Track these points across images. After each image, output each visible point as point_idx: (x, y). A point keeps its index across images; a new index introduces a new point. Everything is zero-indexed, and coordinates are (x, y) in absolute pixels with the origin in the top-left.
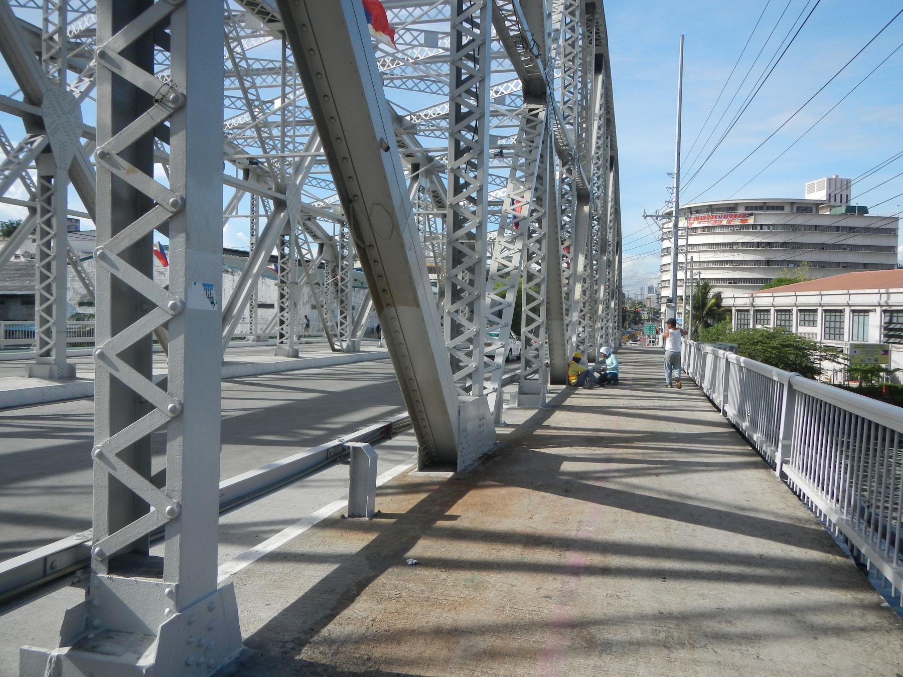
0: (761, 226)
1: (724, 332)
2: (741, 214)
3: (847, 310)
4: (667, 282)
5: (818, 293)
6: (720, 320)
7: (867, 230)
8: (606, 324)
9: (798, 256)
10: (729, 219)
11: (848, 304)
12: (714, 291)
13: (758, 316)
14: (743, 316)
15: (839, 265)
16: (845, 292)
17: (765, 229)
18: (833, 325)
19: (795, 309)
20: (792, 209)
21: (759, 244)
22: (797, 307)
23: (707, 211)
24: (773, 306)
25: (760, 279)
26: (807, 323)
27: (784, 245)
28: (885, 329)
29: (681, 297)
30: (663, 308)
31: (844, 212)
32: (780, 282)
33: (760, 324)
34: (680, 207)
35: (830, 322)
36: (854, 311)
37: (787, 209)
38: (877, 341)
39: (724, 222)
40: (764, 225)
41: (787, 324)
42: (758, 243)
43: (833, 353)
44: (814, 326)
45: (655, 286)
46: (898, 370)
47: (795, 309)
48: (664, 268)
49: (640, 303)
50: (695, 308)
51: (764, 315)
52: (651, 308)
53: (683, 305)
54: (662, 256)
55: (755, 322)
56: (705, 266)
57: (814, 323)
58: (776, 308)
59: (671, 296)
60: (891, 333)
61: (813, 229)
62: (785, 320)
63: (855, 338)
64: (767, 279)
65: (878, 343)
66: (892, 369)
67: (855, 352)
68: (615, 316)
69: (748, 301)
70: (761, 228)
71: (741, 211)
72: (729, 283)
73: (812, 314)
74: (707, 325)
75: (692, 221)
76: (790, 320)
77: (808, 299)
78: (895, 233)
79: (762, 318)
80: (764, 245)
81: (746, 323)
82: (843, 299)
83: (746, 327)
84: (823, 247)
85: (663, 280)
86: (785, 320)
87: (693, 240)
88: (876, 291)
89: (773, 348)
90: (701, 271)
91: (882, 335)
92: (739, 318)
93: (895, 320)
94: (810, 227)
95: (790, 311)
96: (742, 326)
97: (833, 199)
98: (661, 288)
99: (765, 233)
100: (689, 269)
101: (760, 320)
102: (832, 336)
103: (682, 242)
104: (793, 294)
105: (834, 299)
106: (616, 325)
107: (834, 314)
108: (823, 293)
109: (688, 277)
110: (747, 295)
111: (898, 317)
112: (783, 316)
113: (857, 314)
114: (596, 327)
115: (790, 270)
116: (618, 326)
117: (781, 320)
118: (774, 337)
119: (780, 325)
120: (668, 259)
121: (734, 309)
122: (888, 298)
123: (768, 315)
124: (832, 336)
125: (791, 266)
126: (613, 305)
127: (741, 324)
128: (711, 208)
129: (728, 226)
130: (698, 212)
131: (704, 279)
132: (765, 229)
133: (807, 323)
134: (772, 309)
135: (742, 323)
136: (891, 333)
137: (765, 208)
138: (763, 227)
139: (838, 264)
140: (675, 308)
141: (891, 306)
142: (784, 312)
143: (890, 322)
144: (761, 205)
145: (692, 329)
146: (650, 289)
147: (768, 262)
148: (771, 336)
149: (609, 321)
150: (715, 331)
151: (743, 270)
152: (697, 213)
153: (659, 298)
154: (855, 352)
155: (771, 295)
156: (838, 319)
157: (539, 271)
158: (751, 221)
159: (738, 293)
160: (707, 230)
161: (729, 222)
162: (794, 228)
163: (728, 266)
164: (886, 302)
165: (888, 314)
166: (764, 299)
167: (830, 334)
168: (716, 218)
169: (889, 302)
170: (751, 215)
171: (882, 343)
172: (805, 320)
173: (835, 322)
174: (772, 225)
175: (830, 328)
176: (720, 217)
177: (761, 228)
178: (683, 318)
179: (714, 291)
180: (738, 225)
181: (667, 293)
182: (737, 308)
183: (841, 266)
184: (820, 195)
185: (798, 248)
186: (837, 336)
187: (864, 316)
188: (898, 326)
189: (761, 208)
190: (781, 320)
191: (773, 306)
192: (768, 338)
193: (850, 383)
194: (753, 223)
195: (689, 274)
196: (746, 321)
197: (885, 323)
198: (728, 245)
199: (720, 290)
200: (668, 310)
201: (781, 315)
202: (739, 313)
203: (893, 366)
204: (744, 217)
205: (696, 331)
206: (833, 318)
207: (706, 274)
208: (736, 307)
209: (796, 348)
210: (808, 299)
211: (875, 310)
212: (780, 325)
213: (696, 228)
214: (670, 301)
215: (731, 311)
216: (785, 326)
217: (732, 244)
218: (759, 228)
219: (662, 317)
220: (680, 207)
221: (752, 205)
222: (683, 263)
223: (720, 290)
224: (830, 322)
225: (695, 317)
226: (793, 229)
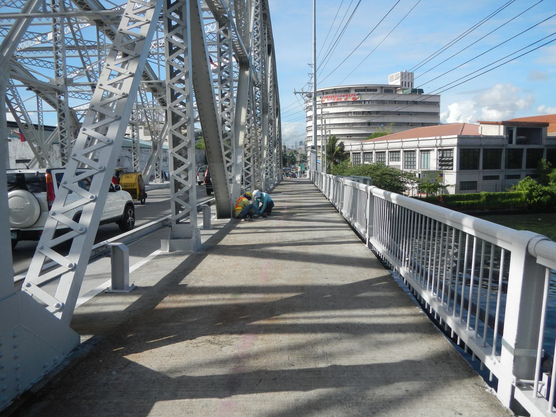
0: (365, 101)
1: (347, 167)
2: (352, 94)
3: (418, 150)
4: (311, 138)
5: (400, 140)
6: (343, 160)
7: (423, 103)
8: (270, 165)
9: (386, 119)
10: (346, 97)
11: (418, 146)
12: (339, 142)
13: (366, 156)
14: (356, 156)
16: (416, 139)
18: (409, 160)
19: (387, 151)
20: (382, 91)
21: (363, 113)
22: (388, 149)
23: (333, 93)
24: (374, 149)
25: (364, 134)
26: (394, 159)
27: (377, 113)
28: (440, 161)
29: (320, 146)
30: (309, 154)
31: (410, 92)
32: (376, 135)
34: (317, 91)
35: (408, 158)
36: (421, 151)
37: (379, 91)
38: (435, 168)
39: (343, 100)
40: (366, 101)
41: (383, 160)
42: (363, 112)
43: (411, 176)
44: (398, 161)
45: (304, 141)
46: (448, 185)
47: (387, 151)
49: (295, 151)
50: (328, 152)
51: (369, 155)
52: (302, 154)
53: (321, 151)
54: (307, 121)
55: (364, 160)
56: (332, 127)
57: (398, 159)
58: (376, 151)
59: (313, 145)
60: (443, 163)
61: (394, 102)
62: (382, 158)
63: (422, 167)
64: (369, 134)
65: (436, 170)
66: (445, 185)
67: (424, 176)
68: (278, 159)
69: (359, 147)
71: (353, 92)
72: (347, 137)
73: (397, 153)
74: (336, 163)
75: (324, 99)
76: (384, 158)
77: (395, 144)
78: (438, 105)
79: (368, 157)
80: (366, 113)
81: (358, 161)
82: (415, 144)
83: (358, 163)
84: (399, 114)
85: (308, 136)
86: (382, 158)
87: (325, 110)
88: (434, 138)
89: (378, 176)
90: (331, 130)
91: (438, 165)
92: (354, 158)
93: (445, 155)
94: (392, 101)
95: (384, 152)
96: (357, 163)
97: (404, 83)
100: (324, 129)
102: (409, 167)
103: (319, 112)
104: (386, 141)
105: (410, 143)
106: (279, 165)
107: (410, 153)
108: (403, 140)
109: (324, 134)
110: (359, 144)
111: (447, 153)
112: (380, 156)
113: (423, 152)
114: (261, 167)
115: (382, 127)
116: (280, 166)
117: (379, 158)
118: (378, 169)
119: (379, 161)
120: (311, 123)
121: (351, 152)
122: (441, 142)
123: (371, 155)
124: (409, 167)
125: (382, 125)
126: (275, 151)
127: (355, 162)
128: (335, 91)
130: (327, 93)
131: (332, 135)
132: (367, 103)
133: (394, 159)
134: (374, 152)
135: (356, 161)
136: (443, 163)
137: (366, 90)
139: (408, 124)
140: (316, 153)
141: (442, 147)
142: (381, 153)
143: (442, 157)
144: (364, 88)
145: (326, 166)
146: (301, 143)
147: (369, 124)
148: (376, 168)
149: (273, 162)
150: (341, 166)
151: (355, 128)
152: (327, 94)
153: (306, 147)
154: (424, 176)
155: (373, 142)
156: (412, 156)
157: (230, 131)
159: (353, 143)
160: (333, 104)
162: (383, 102)
163: (346, 126)
164: (440, 145)
165: (441, 152)
166: (369, 146)
167: (408, 165)
168: (338, 97)
169: (442, 144)
171: (438, 170)
172: (393, 158)
173: (411, 158)
174: (370, 101)
175: (408, 162)
178: (321, 160)
179: (339, 142)
180: (351, 101)
181: (310, 144)
182: (353, 152)
183: (409, 125)
184: (398, 83)
186: (412, 167)
188: (447, 159)
189: (364, 90)
190: (379, 158)
191: (374, 149)
192: (374, 170)
193: (422, 195)
195: (324, 131)
196: (359, 160)
197: (439, 157)
199: (342, 141)
200: (312, 154)
201: (379, 155)
202: (354, 155)
203: (446, 184)
205: (329, 167)
206: (409, 156)
207: (334, 132)
208: (352, 151)
209: (391, 175)
210: (395, 144)
211: (434, 149)
212: (379, 161)
213: (326, 103)
214: (313, 148)
215: (349, 154)
216: (381, 161)
217: (348, 113)
218: (363, 102)
219: (308, 159)
220: (317, 91)
222: (320, 125)
223: (342, 141)
224: (408, 158)
225: (328, 158)
226: (383, 103)
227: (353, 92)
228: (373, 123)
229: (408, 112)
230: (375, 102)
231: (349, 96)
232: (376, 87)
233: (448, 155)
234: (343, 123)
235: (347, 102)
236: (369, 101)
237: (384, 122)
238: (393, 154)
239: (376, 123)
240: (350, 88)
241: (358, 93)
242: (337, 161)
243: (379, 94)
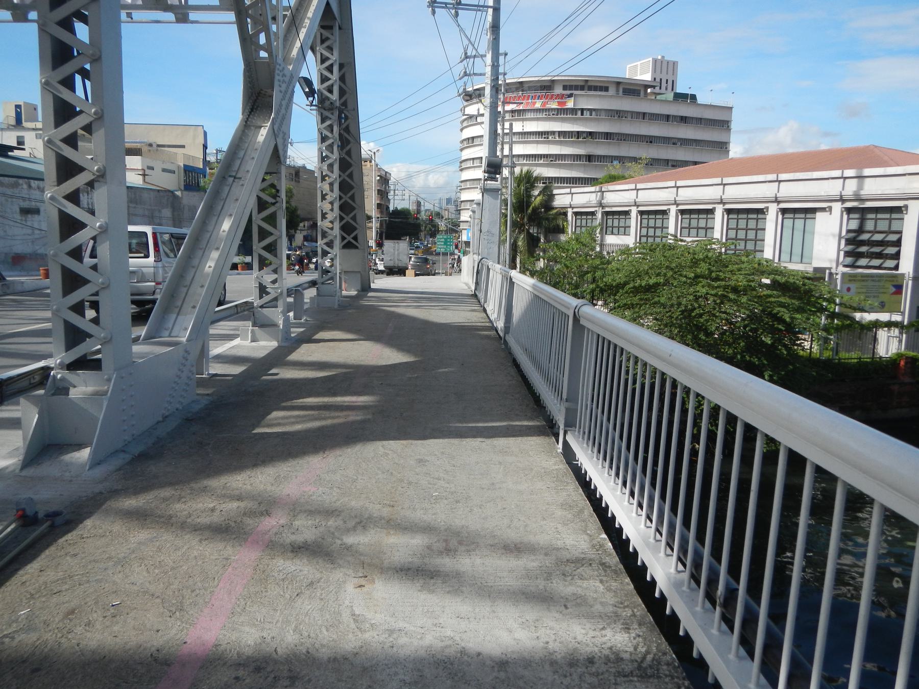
0: (582, 110)
2: (558, 95)
9: (626, 150)
13: (610, 222)
14: (584, 222)
15: (668, 164)
17: (587, 115)
21: (579, 134)
27: (608, 135)
33: (612, 233)
35: (737, 229)
39: (538, 105)
40: (586, 109)
48: (464, 165)
62: (655, 228)
70: (582, 114)
71: (558, 90)
80: (585, 135)
86: (655, 228)
92: (578, 224)
93: (870, 225)
94: (638, 113)
95: (665, 213)
98: (461, 190)
99: (586, 119)
101: (613, 227)
111: (876, 220)
117: (648, 227)
129: (543, 109)
132: (587, 115)
137: (586, 88)
138: (585, 112)
139: (667, 161)
144: (582, 84)
147: (589, 158)
151: (560, 166)
156: (752, 224)
158: (570, 104)
161: (544, 104)
162: (619, 114)
163: (541, 162)
165: (857, 216)
168: (528, 99)
170: (570, 96)
172: (689, 228)
173: (747, 229)
176: (533, 98)
177: (582, 114)
185: (624, 140)
187: (805, 219)
190: (648, 227)
194: (572, 107)
197: (849, 231)
198: (542, 135)
204: (562, 99)
218: (579, 113)
221: (572, 84)
224: (737, 229)
225: (515, 224)
226: (619, 116)
227: (558, 90)
228: (598, 156)
229: (669, 138)
230: (603, 113)
231: (551, 98)
232: (608, 81)
233: (883, 226)
234: (535, 155)
235: (546, 110)
236: (590, 110)
237: (620, 157)
238: (690, 219)
239: (604, 156)
240: (553, 81)
241: (568, 92)
242: (531, 231)
243: (611, 96)
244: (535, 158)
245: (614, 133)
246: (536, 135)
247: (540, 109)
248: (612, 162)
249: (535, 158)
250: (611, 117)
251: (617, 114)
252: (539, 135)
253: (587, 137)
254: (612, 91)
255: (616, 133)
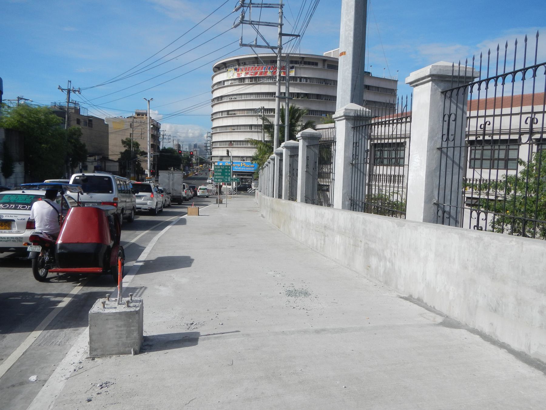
0: (301, 78)
17: (304, 81)
27: (318, 96)
42: (298, 94)
70: (300, 81)
132: (304, 81)
137: (303, 62)
138: (302, 79)
158: (292, 74)
168: (262, 69)
177: (300, 81)
185: (329, 100)
194: (294, 75)
218: (298, 80)
226: (326, 83)
239: (316, 111)
244: (268, 111)
245: (322, 95)
246: (268, 95)
247: (270, 77)
248: (321, 115)
249: (268, 111)
250: (320, 83)
251: (324, 81)
252: (270, 95)
253: (304, 96)
254: (320, 66)
255: (324, 95)
